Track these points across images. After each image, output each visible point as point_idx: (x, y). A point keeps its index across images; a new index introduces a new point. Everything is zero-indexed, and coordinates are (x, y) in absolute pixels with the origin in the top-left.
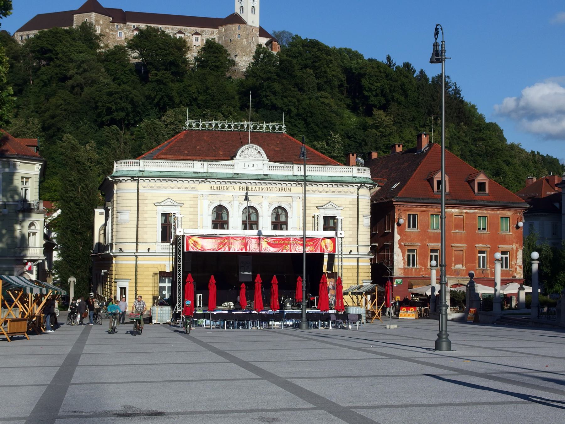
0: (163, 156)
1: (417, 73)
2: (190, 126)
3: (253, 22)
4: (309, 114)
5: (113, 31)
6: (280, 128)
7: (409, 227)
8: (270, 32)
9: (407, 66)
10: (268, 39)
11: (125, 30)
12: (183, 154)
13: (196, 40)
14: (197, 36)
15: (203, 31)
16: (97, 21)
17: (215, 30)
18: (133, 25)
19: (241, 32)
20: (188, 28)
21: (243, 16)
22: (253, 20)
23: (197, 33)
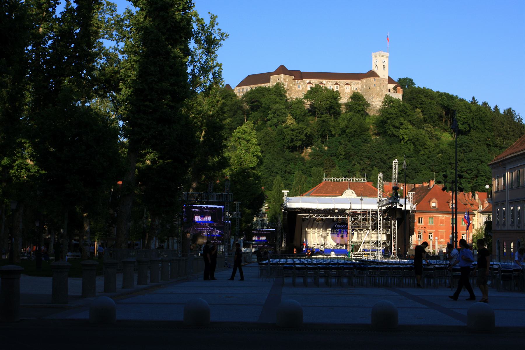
0: (314, 194)
1: (492, 108)
2: (326, 180)
3: (384, 76)
4: (416, 140)
5: (294, 85)
6: (364, 180)
7: (419, 222)
8: (396, 79)
9: (485, 104)
10: (395, 85)
11: (302, 84)
12: (322, 193)
13: (345, 91)
14: (347, 86)
15: (351, 83)
16: (285, 80)
17: (359, 81)
18: (308, 81)
19: (375, 83)
20: (342, 81)
21: (378, 72)
22: (383, 74)
23: (347, 84)
